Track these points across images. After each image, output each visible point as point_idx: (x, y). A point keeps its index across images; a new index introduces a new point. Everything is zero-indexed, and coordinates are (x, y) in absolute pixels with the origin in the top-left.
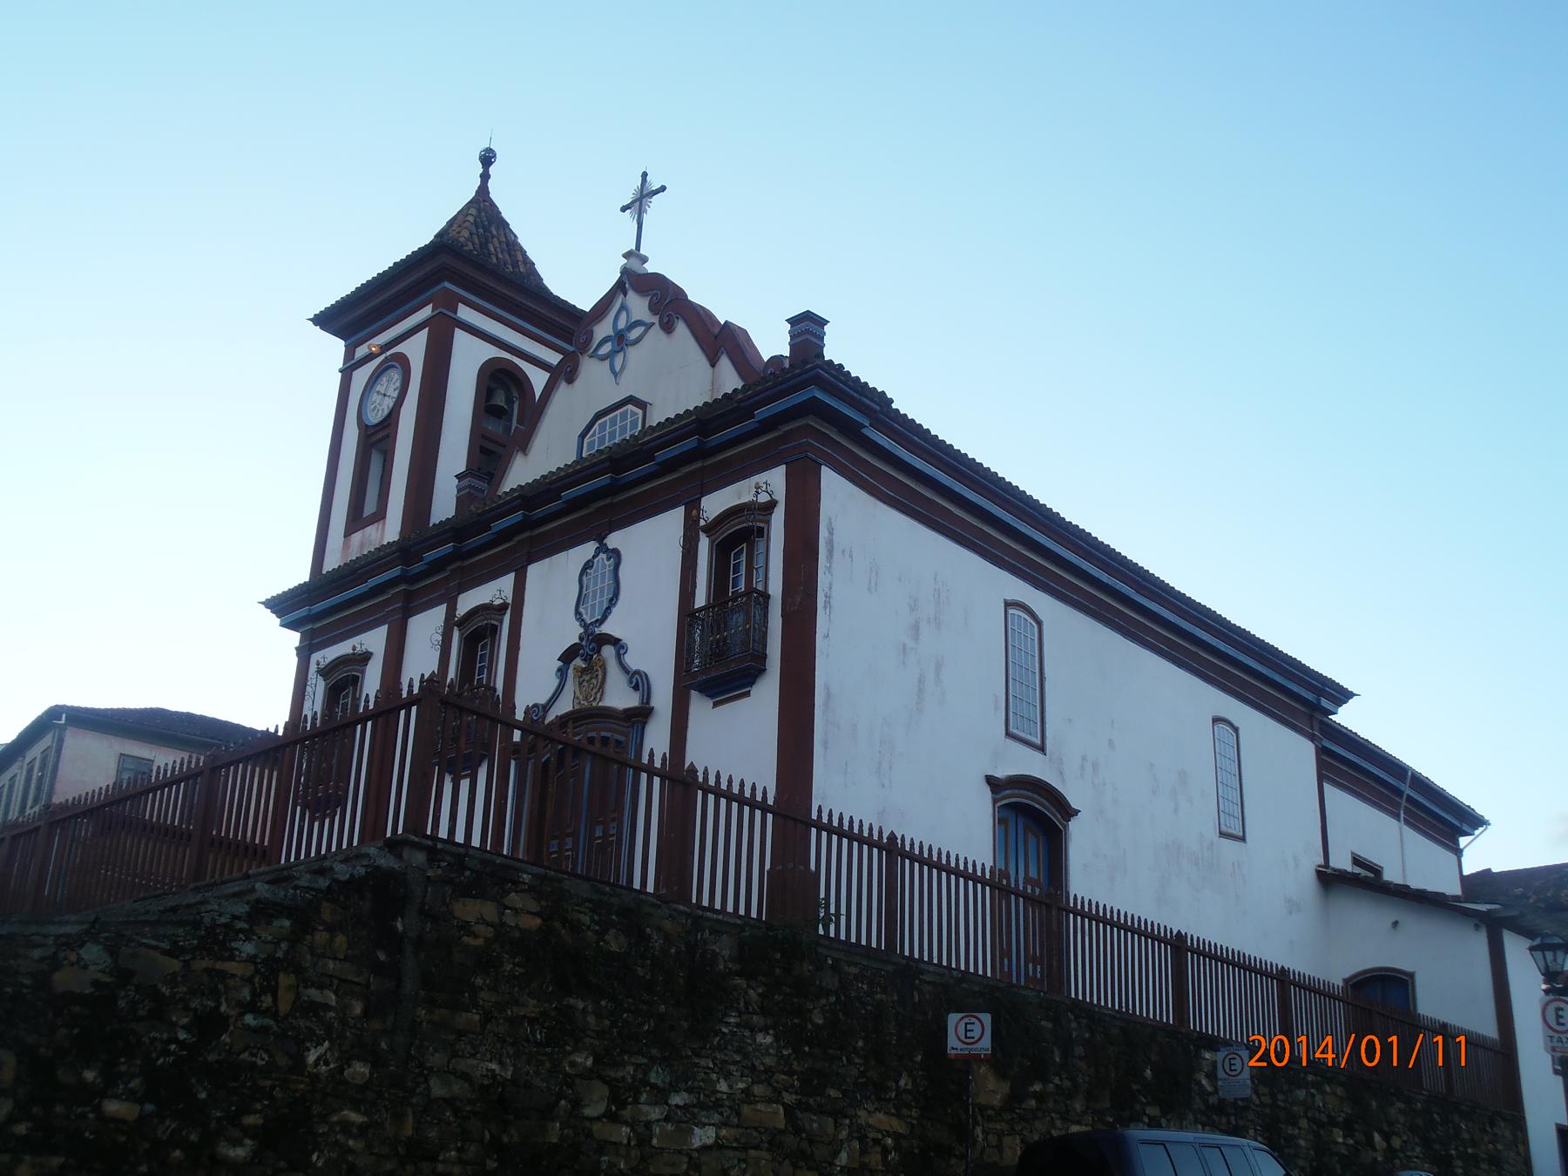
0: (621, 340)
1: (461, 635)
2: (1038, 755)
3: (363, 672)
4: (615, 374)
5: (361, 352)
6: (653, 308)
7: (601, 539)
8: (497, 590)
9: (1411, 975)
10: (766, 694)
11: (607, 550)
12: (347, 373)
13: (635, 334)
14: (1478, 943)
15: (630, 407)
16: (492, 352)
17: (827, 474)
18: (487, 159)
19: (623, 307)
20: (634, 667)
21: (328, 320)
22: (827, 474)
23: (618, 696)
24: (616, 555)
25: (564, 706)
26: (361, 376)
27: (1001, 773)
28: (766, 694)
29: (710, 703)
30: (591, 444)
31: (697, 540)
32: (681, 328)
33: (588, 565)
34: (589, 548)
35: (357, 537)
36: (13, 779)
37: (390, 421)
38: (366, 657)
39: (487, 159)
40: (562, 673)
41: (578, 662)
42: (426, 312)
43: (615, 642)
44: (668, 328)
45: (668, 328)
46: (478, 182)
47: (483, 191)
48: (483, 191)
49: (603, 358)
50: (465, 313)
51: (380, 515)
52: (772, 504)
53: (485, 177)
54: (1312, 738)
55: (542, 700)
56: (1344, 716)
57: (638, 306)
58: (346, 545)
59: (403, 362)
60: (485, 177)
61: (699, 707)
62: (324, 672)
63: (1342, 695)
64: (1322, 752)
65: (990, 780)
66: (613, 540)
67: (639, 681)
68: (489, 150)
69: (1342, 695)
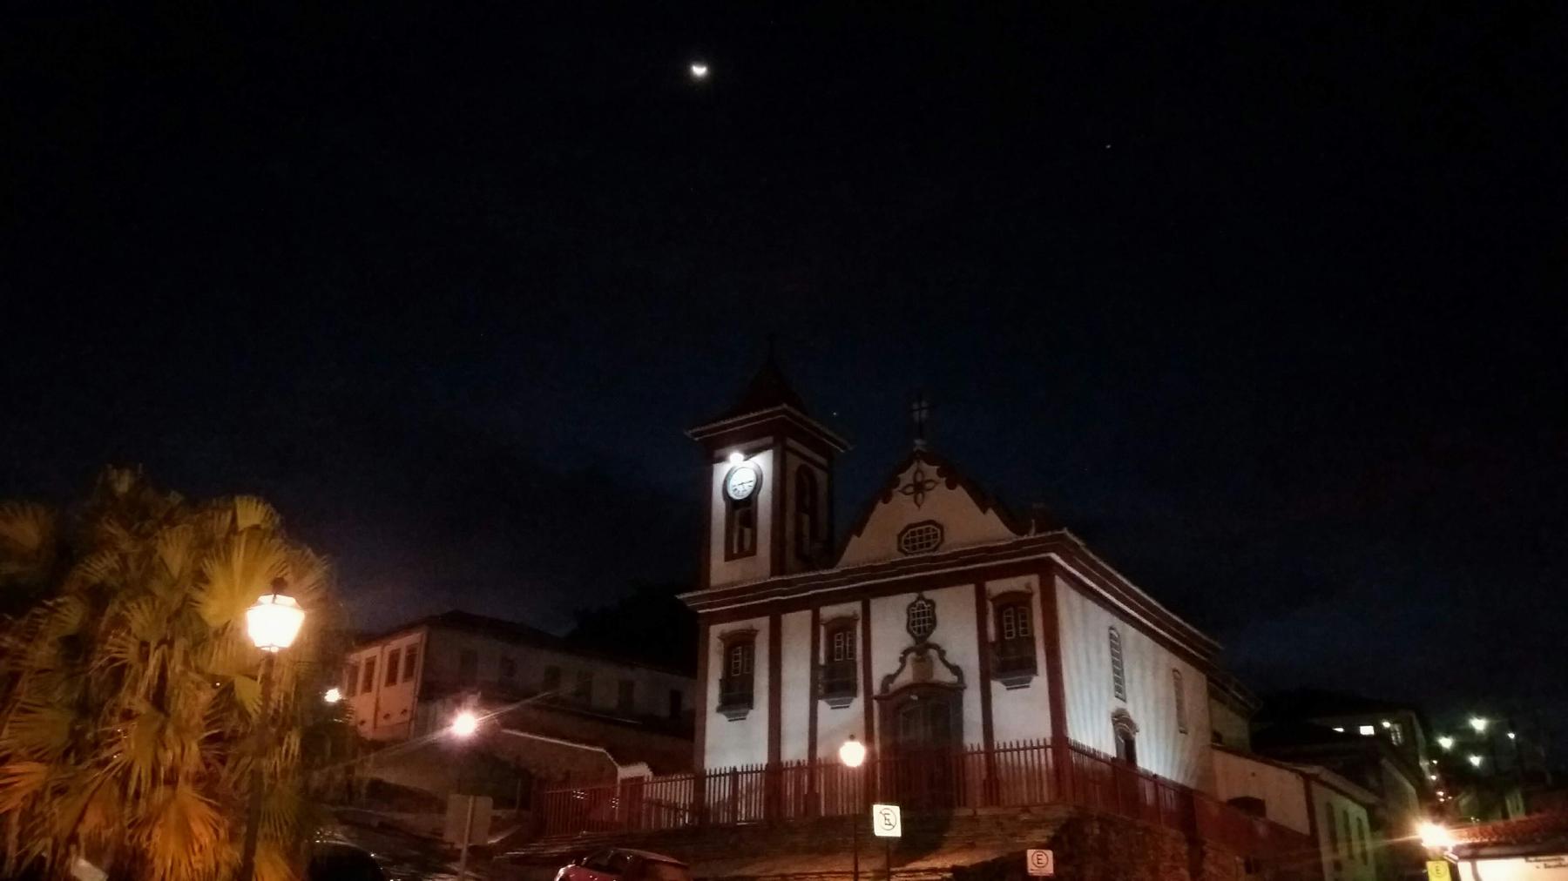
0: (919, 488)
10: (1040, 681)
13: (929, 485)
16: (800, 462)
19: (919, 471)
23: (944, 676)
24: (932, 603)
25: (907, 677)
28: (1040, 681)
33: (913, 605)
34: (910, 598)
36: (371, 664)
40: (903, 660)
41: (912, 655)
43: (936, 647)
44: (951, 486)
51: (753, 551)
52: (1030, 595)
55: (892, 671)
61: (997, 686)
62: (723, 637)
66: (928, 594)
67: (956, 670)
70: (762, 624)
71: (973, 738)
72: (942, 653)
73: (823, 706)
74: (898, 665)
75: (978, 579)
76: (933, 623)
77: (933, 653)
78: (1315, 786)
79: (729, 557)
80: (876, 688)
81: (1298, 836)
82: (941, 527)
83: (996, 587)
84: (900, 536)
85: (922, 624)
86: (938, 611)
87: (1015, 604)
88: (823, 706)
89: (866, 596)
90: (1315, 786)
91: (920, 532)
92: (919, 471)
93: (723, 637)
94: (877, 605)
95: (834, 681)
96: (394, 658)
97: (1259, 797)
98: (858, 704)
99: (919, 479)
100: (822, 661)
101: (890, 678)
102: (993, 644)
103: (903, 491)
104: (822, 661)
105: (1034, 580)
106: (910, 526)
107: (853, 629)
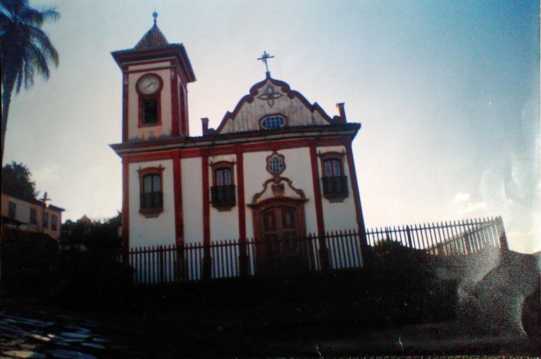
0: (270, 96)
4: (271, 106)
5: (131, 68)
6: (283, 90)
8: (231, 158)
10: (351, 200)
11: (277, 154)
13: (276, 96)
18: (155, 15)
23: (289, 193)
24: (282, 156)
25: (269, 194)
26: (134, 78)
28: (351, 200)
30: (264, 124)
31: (316, 159)
32: (296, 98)
34: (270, 153)
38: (163, 169)
39: (155, 15)
40: (265, 185)
41: (271, 183)
43: (287, 180)
46: (153, 23)
47: (155, 26)
48: (155, 26)
49: (264, 99)
53: (155, 21)
55: (259, 191)
57: (278, 89)
59: (160, 79)
60: (155, 21)
62: (140, 171)
66: (280, 152)
67: (300, 192)
68: (155, 13)
71: (312, 227)
72: (290, 183)
73: (213, 212)
74: (262, 188)
75: (312, 144)
76: (284, 166)
80: (248, 200)
84: (260, 121)
85: (276, 167)
86: (286, 161)
88: (213, 212)
89: (239, 150)
91: (273, 119)
93: (140, 171)
94: (246, 156)
95: (222, 195)
98: (235, 210)
100: (211, 184)
101: (257, 196)
103: (259, 98)
104: (211, 184)
107: (231, 170)
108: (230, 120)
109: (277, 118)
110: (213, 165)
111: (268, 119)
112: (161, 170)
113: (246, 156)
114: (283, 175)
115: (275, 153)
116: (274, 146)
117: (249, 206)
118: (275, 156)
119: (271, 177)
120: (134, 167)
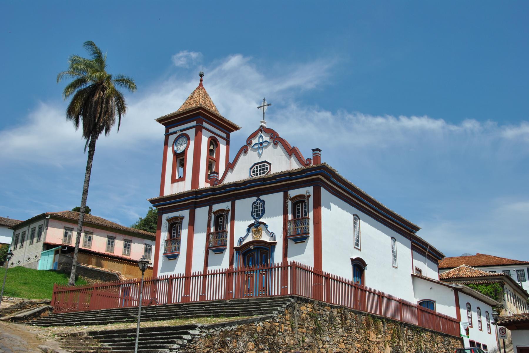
1: (215, 216)
2: (359, 251)
3: (182, 222)
5: (171, 130)
6: (271, 138)
7: (258, 196)
8: (226, 205)
9: (435, 302)
11: (260, 200)
12: (167, 135)
14: (453, 294)
15: (265, 164)
17: (322, 189)
20: (271, 232)
21: (160, 120)
22: (322, 189)
23: (265, 238)
25: (250, 239)
26: (172, 138)
27: (354, 258)
29: (294, 242)
33: (254, 203)
34: (254, 199)
35: (175, 184)
37: (184, 153)
40: (248, 230)
42: (194, 123)
43: (264, 224)
45: (276, 144)
50: (205, 124)
52: (309, 196)
53: (201, 81)
54: (410, 240)
55: (243, 236)
56: (418, 234)
57: (267, 138)
58: (172, 187)
62: (168, 220)
63: (417, 229)
64: (412, 242)
65: (352, 260)
66: (262, 197)
67: (272, 235)
69: (417, 229)
70: (186, 213)
77: (262, 226)
78: (460, 294)
79: (174, 181)
80: (236, 245)
81: (451, 320)
82: (270, 164)
83: (293, 193)
84: (251, 169)
87: (299, 203)
90: (460, 294)
91: (260, 167)
92: (261, 136)
93: (168, 220)
94: (237, 202)
96: (33, 230)
97: (434, 300)
99: (261, 141)
101: (241, 240)
102: (289, 221)
105: (310, 190)
106: (255, 164)
108: (230, 170)
109: (264, 166)
110: (214, 213)
111: (257, 167)
112: (182, 218)
113: (237, 202)
114: (260, 220)
115: (259, 199)
116: (258, 193)
117: (236, 248)
118: (259, 201)
119: (252, 222)
120: (165, 217)
